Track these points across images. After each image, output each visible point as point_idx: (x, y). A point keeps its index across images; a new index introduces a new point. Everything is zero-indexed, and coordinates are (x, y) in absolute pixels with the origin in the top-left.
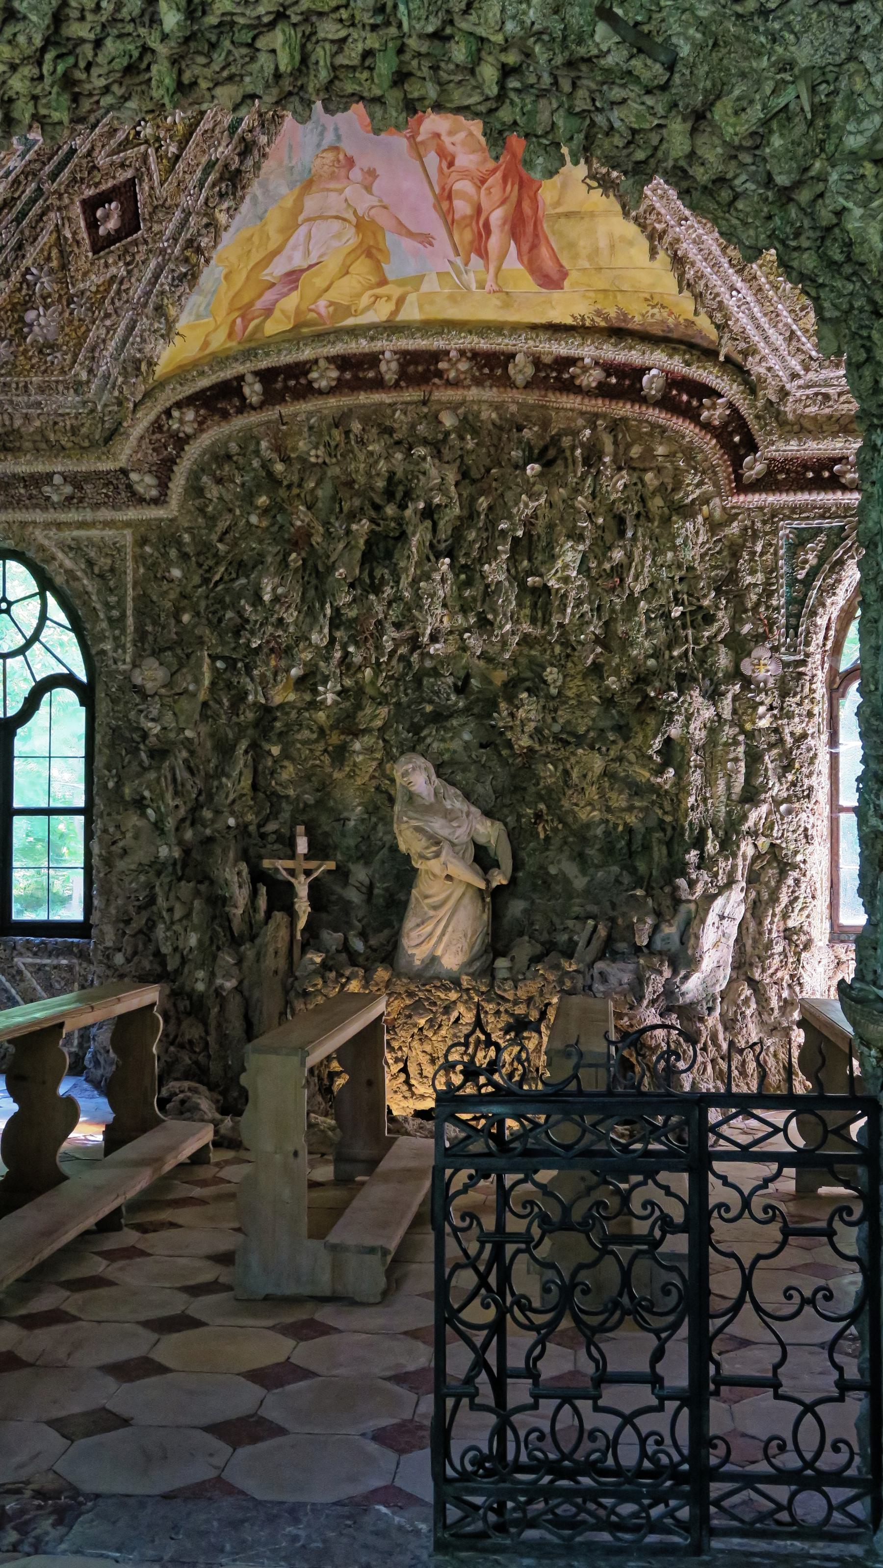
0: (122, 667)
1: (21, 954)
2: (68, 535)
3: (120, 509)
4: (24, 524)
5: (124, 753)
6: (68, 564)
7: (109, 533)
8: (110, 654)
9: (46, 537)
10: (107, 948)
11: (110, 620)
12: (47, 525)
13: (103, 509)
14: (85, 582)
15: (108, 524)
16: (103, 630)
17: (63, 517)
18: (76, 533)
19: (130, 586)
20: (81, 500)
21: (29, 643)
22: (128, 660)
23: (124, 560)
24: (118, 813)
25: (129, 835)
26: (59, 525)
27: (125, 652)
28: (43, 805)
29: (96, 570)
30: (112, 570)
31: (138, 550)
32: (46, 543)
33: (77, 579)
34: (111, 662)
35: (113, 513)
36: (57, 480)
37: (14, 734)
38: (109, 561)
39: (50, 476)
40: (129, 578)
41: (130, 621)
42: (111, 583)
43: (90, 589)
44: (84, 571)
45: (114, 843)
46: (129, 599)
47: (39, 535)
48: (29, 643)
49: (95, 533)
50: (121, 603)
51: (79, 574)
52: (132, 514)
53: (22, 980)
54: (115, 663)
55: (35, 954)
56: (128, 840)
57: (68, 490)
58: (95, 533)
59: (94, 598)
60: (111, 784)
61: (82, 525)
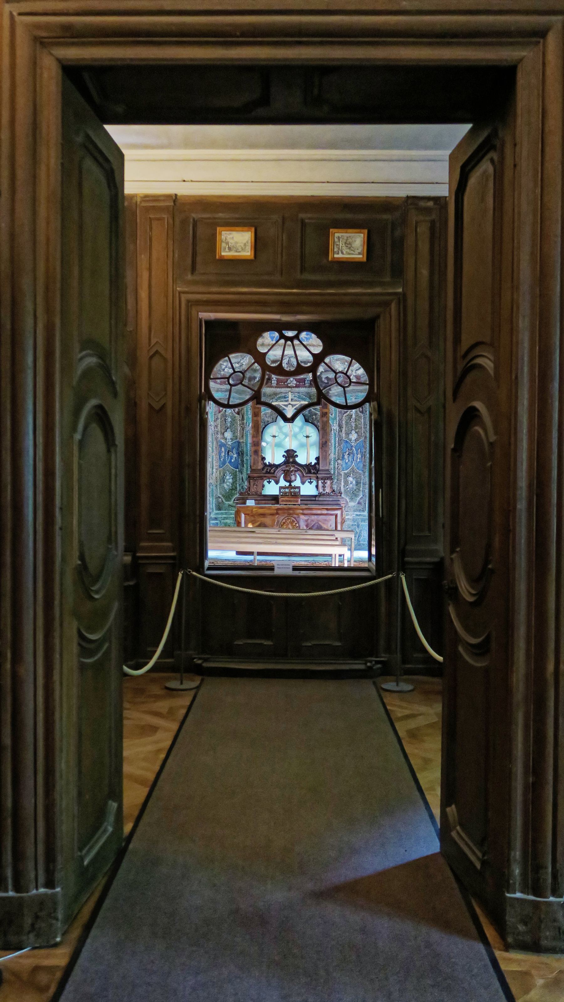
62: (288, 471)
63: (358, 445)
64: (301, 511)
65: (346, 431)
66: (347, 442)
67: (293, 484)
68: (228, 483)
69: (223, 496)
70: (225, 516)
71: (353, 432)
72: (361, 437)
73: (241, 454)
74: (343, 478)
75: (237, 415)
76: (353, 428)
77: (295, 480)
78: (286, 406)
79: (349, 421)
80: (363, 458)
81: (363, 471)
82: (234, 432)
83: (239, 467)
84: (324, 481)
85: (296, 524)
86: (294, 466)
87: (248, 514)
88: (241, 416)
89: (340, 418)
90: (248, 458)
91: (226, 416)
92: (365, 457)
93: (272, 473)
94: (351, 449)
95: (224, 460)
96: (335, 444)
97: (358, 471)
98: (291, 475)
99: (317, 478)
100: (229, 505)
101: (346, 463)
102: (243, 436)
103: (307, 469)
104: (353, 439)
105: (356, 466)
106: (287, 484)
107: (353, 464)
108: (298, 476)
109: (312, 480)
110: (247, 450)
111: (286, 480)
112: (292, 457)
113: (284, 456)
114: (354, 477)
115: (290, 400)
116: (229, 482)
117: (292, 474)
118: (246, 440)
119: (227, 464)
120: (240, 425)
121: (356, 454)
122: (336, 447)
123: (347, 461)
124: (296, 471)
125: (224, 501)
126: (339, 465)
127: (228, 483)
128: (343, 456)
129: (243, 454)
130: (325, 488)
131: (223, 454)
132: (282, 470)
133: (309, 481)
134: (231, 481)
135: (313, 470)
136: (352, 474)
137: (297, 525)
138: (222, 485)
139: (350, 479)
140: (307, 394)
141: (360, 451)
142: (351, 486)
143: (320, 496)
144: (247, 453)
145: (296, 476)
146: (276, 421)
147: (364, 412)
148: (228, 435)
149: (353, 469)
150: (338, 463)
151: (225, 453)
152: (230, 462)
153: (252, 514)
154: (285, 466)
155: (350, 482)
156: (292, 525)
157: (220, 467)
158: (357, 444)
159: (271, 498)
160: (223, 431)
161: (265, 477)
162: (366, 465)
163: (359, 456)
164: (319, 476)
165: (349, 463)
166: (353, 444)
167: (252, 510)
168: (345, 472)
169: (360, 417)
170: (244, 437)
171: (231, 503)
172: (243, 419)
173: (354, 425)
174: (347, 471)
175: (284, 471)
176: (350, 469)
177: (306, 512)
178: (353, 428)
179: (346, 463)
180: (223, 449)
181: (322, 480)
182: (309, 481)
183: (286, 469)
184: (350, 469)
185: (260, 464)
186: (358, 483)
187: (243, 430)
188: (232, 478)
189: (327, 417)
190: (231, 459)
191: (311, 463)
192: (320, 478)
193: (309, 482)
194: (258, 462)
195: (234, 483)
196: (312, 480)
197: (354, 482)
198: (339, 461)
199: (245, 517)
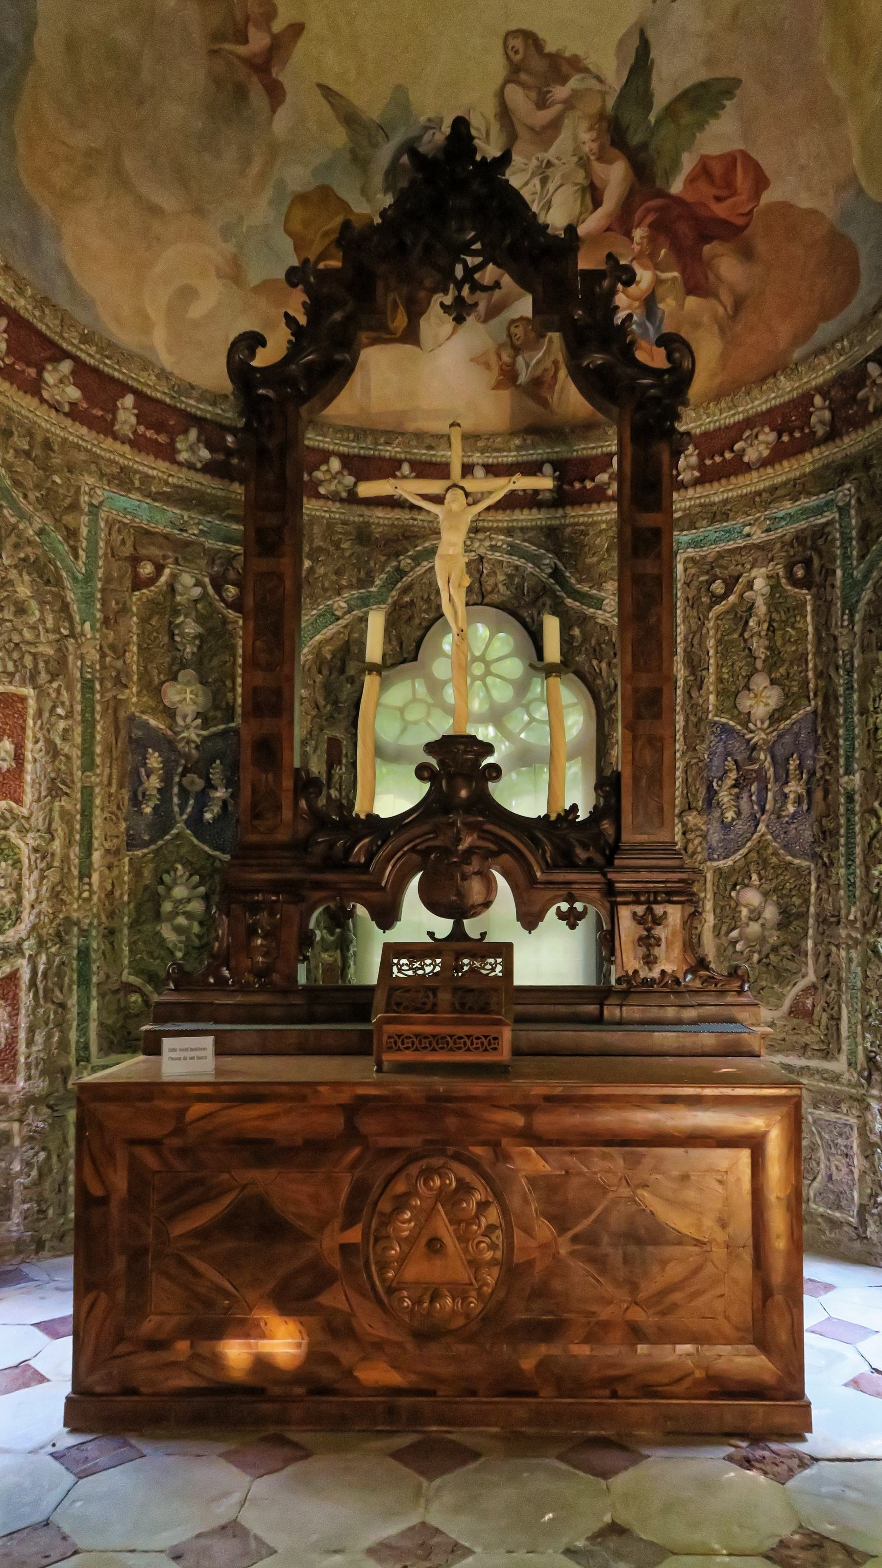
62: (446, 852)
63: (788, 739)
64: (518, 1120)
65: (720, 680)
66: (726, 729)
67: (473, 928)
71: (760, 681)
72: (804, 701)
74: (710, 895)
76: (759, 664)
77: (487, 904)
78: (438, 500)
79: (736, 636)
80: (819, 795)
81: (815, 857)
84: (650, 910)
85: (483, 1206)
87: (154, 1144)
89: (694, 627)
92: (826, 792)
94: (751, 760)
97: (789, 858)
98: (464, 878)
99: (610, 891)
101: (726, 827)
103: (555, 846)
105: (775, 839)
106: (443, 927)
107: (762, 828)
108: (502, 882)
109: (579, 906)
111: (434, 906)
114: (767, 887)
115: (456, 470)
117: (469, 869)
121: (776, 780)
122: (678, 755)
123: (730, 815)
124: (489, 855)
126: (690, 836)
128: (711, 793)
130: (656, 951)
132: (413, 849)
133: (564, 906)
135: (585, 847)
136: (755, 877)
137: (493, 1215)
139: (751, 897)
140: (548, 536)
141: (800, 767)
142: (754, 928)
145: (490, 886)
146: (415, 659)
147: (817, 579)
149: (761, 847)
150: (684, 825)
153: (177, 1142)
154: (425, 828)
155: (745, 912)
158: (780, 736)
161: (319, 886)
162: (839, 826)
163: (794, 788)
165: (740, 827)
166: (758, 737)
167: (181, 1114)
168: (721, 864)
173: (761, 653)
174: (729, 862)
175: (425, 853)
176: (744, 851)
177: (544, 1122)
178: (759, 664)
179: (726, 827)
181: (638, 902)
182: (564, 906)
183: (437, 843)
184: (744, 851)
185: (287, 814)
189: (659, 556)
191: (574, 808)
192: (623, 893)
193: (561, 915)
194: (279, 808)
196: (579, 906)
197: (770, 913)
198: (692, 819)
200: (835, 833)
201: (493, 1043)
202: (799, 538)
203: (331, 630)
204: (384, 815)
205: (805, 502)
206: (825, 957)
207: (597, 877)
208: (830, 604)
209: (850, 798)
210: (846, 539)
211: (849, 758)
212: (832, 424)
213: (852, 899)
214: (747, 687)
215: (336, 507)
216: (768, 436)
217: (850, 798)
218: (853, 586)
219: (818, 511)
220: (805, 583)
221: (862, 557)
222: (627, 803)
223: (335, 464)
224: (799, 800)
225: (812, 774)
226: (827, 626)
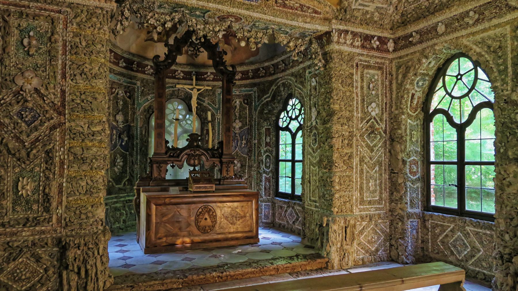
0: (506, 93)
1: (468, 226)
2: (478, 37)
3: (502, 17)
4: (457, 38)
5: (508, 134)
6: (478, 50)
7: (498, 31)
8: (500, 87)
9: (469, 41)
10: (502, 231)
11: (499, 72)
12: (468, 35)
13: (493, 20)
14: (486, 56)
15: (496, 26)
16: (496, 77)
17: (474, 29)
18: (481, 35)
19: (509, 53)
20: (483, 19)
21: (470, 91)
22: (509, 89)
23: (506, 41)
24: (506, 164)
25: (511, 176)
26: (473, 34)
27: (507, 85)
28: (478, 160)
29: (492, 49)
30: (500, 47)
31: (514, 34)
32: (468, 43)
33: (483, 56)
34: (500, 91)
35: (499, 20)
36: (471, 14)
37: (465, 130)
38: (498, 43)
39: (468, 12)
40: (509, 49)
41: (510, 70)
42: (500, 54)
43: (489, 59)
44: (486, 52)
45: (504, 179)
46: (509, 59)
47: (465, 41)
48: (470, 91)
49: (491, 33)
50: (505, 61)
51: (483, 53)
52: (509, 17)
53: (469, 237)
54: (502, 91)
55: (474, 227)
56: (510, 179)
57: (477, 16)
58: (491, 33)
59: (491, 62)
60: (502, 150)
61: (485, 30)
68: (119, 167)
69: (114, 179)
70: (115, 200)
71: (237, 121)
73: (131, 137)
75: (128, 99)
80: (249, 144)
81: (248, 155)
82: (125, 115)
83: (129, 150)
85: (213, 212)
86: (199, 150)
88: (132, 101)
90: (138, 141)
91: (118, 99)
93: (175, 157)
95: (115, 142)
96: (219, 131)
100: (120, 189)
102: (133, 121)
104: (237, 127)
110: (137, 134)
112: (196, 141)
113: (187, 140)
116: (120, 166)
118: (137, 124)
119: (118, 147)
120: (131, 109)
125: (114, 184)
127: (119, 167)
129: (133, 137)
131: (115, 137)
134: (121, 164)
138: (113, 168)
141: (245, 138)
143: (224, 180)
144: (137, 137)
148: (120, 118)
151: (116, 136)
152: (121, 145)
156: (209, 215)
157: (112, 150)
159: (173, 184)
160: (115, 113)
163: (244, 142)
164: (224, 160)
166: (236, 132)
169: (246, 108)
170: (135, 121)
171: (121, 186)
172: (134, 104)
180: (115, 132)
186: (242, 166)
187: (134, 115)
188: (123, 162)
190: (122, 142)
195: (124, 167)
199: (156, 208)
200: (252, 151)
201: (212, 187)
202: (246, 95)
203: (147, 104)
204: (180, 147)
205: (247, 89)
206: (249, 173)
207: (219, 159)
208: (252, 109)
209: (255, 144)
210: (255, 97)
211: (255, 138)
212: (253, 76)
213: (255, 163)
214: (235, 122)
215: (149, 76)
216: (240, 75)
217: (255, 144)
218: (256, 107)
219: (250, 91)
220: (247, 104)
221: (258, 102)
222: (224, 146)
223: (149, 67)
224: (245, 144)
225: (247, 139)
226: (251, 113)
